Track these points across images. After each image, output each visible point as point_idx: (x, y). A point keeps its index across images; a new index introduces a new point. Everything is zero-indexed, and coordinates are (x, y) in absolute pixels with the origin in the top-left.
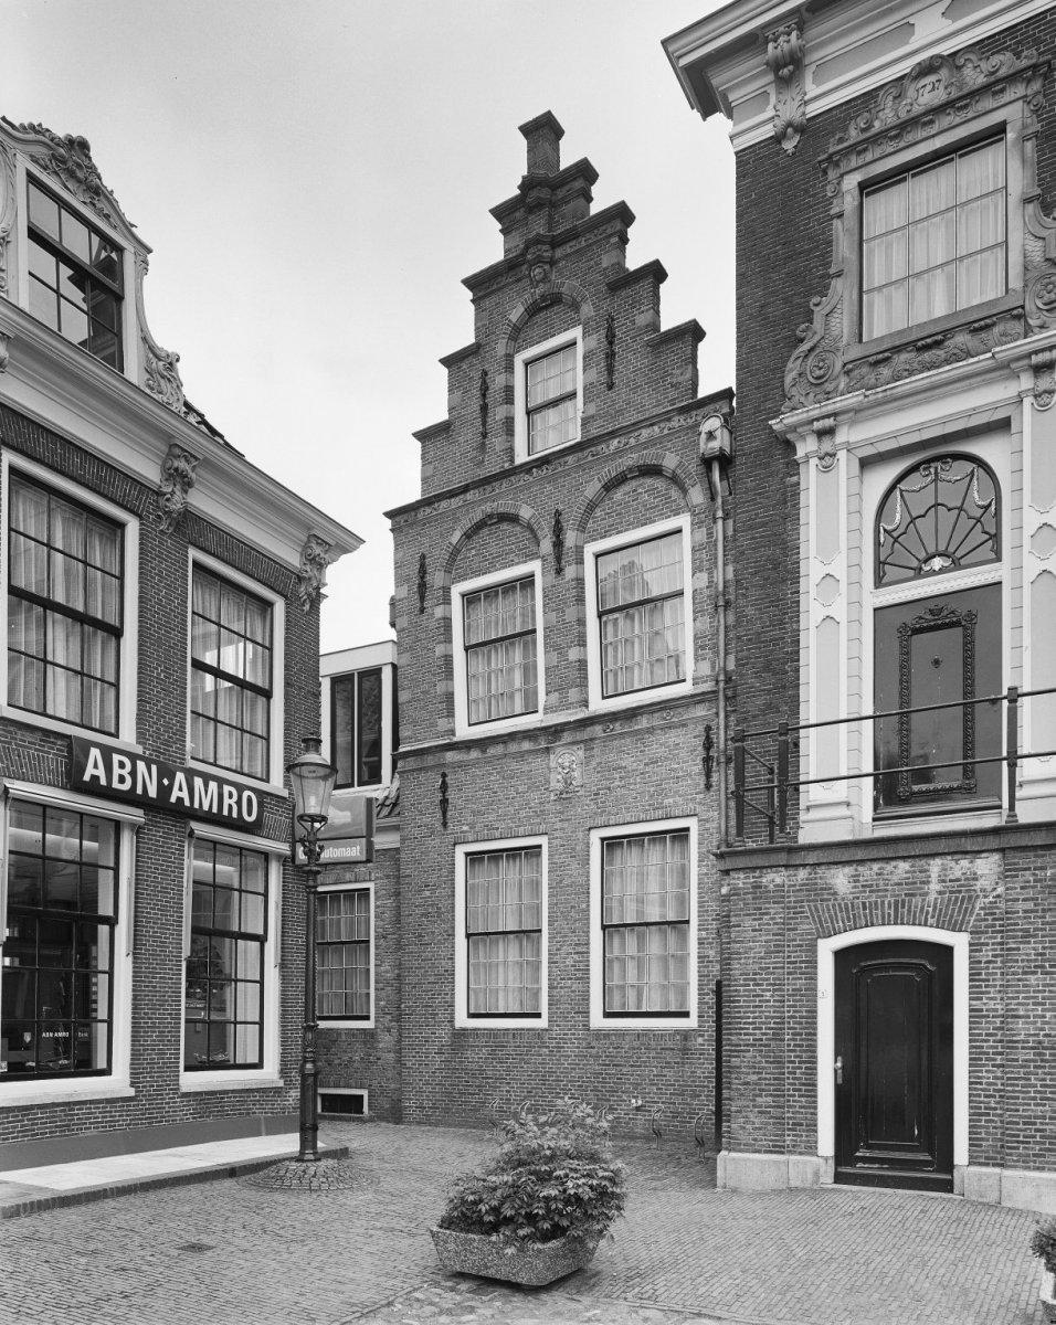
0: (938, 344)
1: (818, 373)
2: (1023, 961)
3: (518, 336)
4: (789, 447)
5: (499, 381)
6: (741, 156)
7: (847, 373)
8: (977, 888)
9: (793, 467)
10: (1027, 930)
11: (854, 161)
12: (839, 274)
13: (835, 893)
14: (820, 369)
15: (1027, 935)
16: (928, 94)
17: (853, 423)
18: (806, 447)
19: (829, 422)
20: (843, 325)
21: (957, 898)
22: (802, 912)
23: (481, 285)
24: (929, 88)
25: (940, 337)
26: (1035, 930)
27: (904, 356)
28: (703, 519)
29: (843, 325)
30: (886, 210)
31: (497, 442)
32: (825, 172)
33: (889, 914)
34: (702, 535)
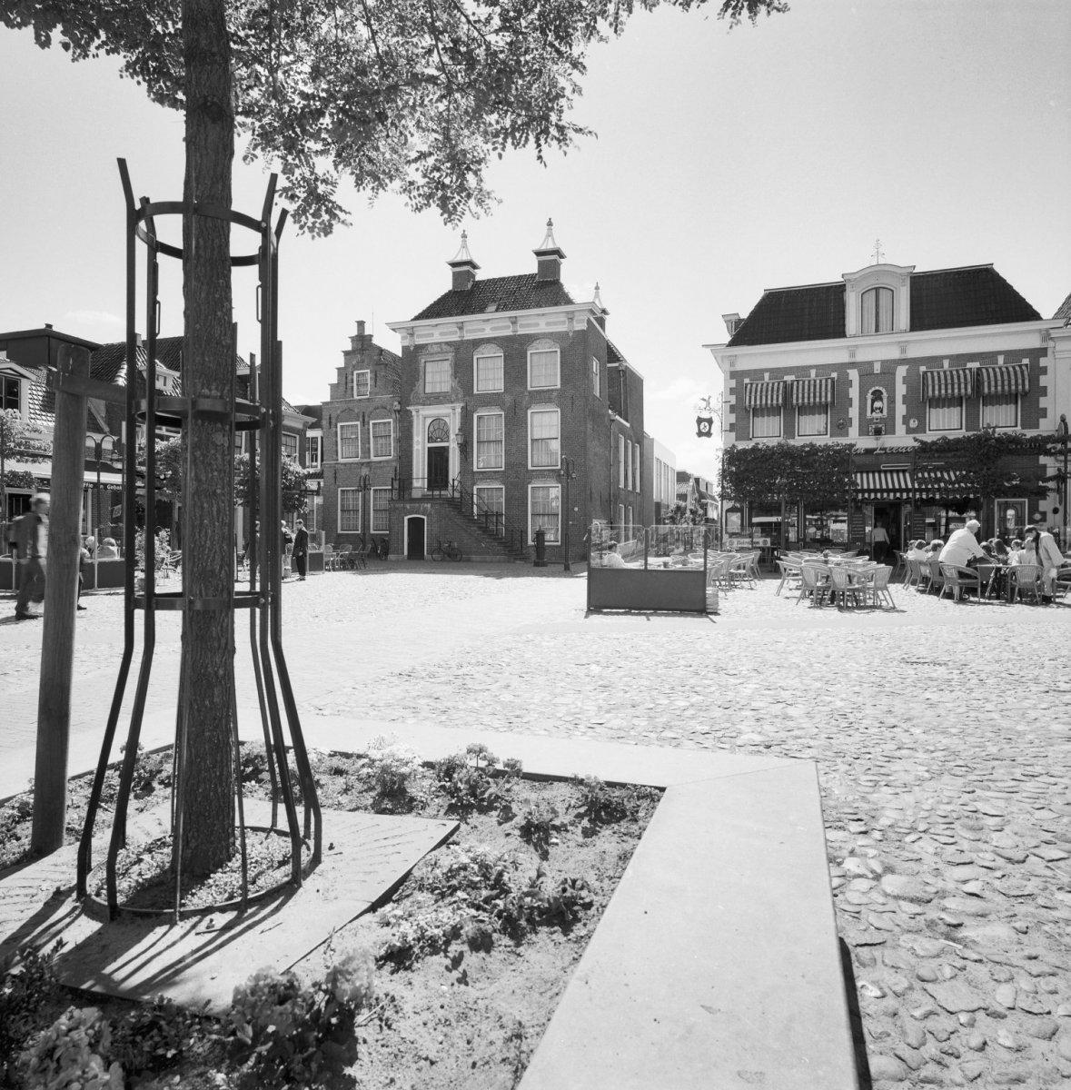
3: (355, 368)
5: (349, 378)
16: (436, 349)
18: (414, 413)
20: (421, 388)
23: (346, 353)
28: (395, 421)
29: (421, 388)
31: (349, 392)
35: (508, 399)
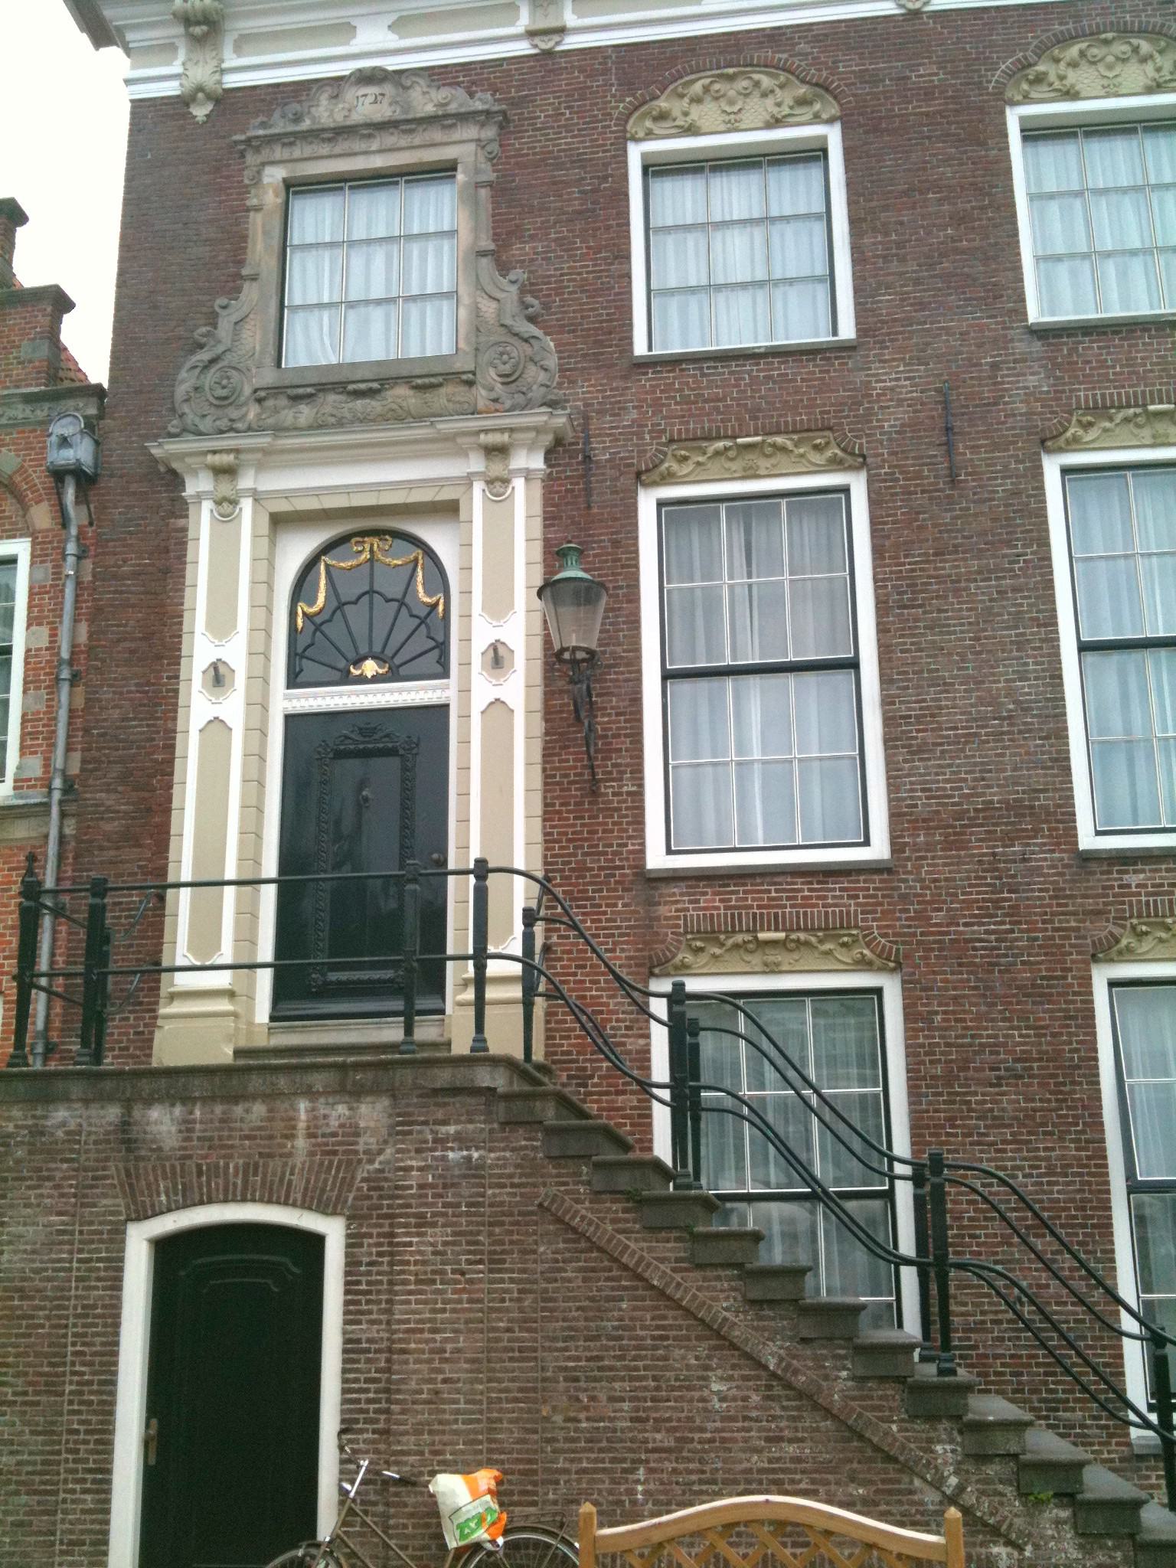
0: (370, 393)
1: (224, 393)
2: (416, 1263)
4: (175, 480)
6: (139, 108)
7: (259, 401)
8: (360, 1148)
9: (179, 508)
10: (422, 1216)
11: (279, 153)
12: (254, 278)
13: (160, 1149)
14: (224, 387)
15: (422, 1222)
16: (366, 106)
17: (260, 467)
18: (198, 484)
19: (229, 459)
20: (254, 338)
21: (331, 1163)
22: (106, 1177)
24: (371, 99)
25: (375, 385)
26: (434, 1215)
27: (332, 397)
28: (45, 552)
29: (254, 338)
30: (315, 219)
32: (242, 155)
33: (235, 1185)
34: (45, 572)
35: (897, 383)
